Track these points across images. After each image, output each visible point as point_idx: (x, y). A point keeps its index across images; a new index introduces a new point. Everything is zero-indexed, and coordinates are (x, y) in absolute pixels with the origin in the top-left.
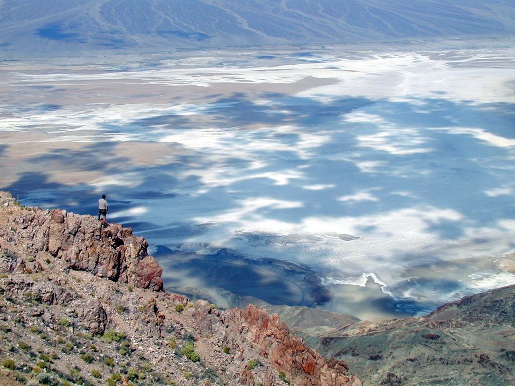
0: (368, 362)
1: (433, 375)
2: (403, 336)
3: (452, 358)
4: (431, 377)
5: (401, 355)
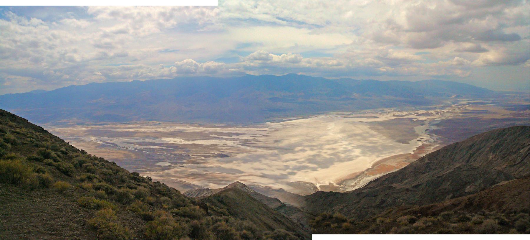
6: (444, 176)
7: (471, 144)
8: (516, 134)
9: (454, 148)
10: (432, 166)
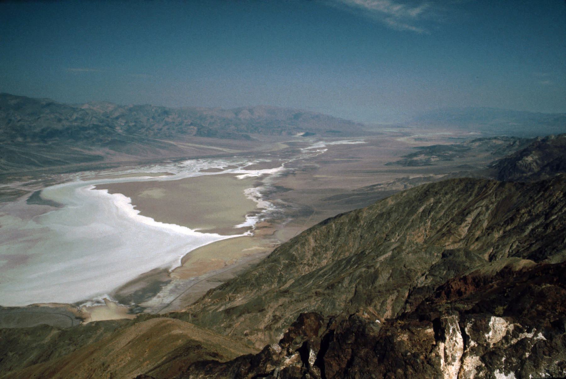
0: (259, 314)
1: (296, 309)
2: (271, 296)
3: (301, 298)
4: (295, 310)
5: (275, 305)
6: (378, 265)
7: (384, 210)
8: (453, 192)
9: (357, 219)
10: (322, 252)
